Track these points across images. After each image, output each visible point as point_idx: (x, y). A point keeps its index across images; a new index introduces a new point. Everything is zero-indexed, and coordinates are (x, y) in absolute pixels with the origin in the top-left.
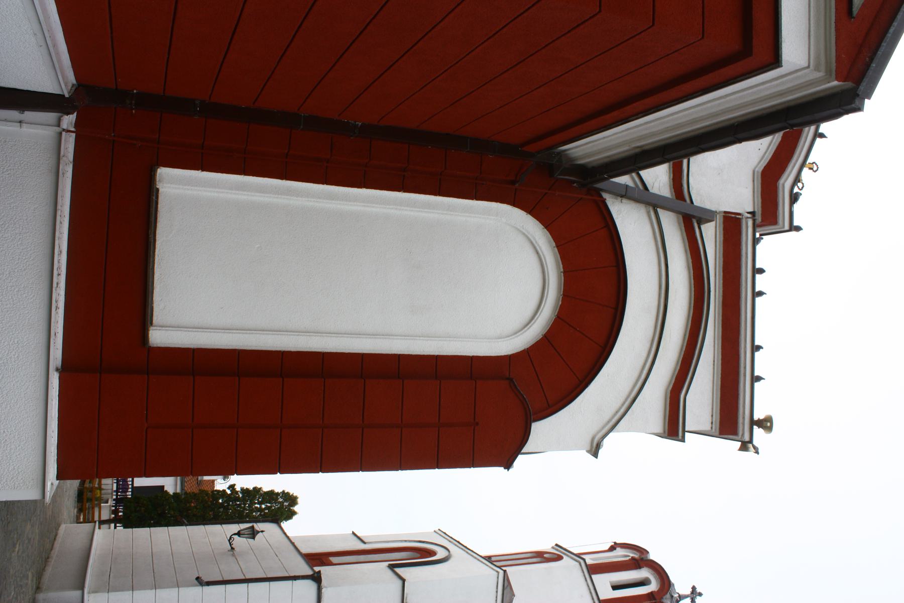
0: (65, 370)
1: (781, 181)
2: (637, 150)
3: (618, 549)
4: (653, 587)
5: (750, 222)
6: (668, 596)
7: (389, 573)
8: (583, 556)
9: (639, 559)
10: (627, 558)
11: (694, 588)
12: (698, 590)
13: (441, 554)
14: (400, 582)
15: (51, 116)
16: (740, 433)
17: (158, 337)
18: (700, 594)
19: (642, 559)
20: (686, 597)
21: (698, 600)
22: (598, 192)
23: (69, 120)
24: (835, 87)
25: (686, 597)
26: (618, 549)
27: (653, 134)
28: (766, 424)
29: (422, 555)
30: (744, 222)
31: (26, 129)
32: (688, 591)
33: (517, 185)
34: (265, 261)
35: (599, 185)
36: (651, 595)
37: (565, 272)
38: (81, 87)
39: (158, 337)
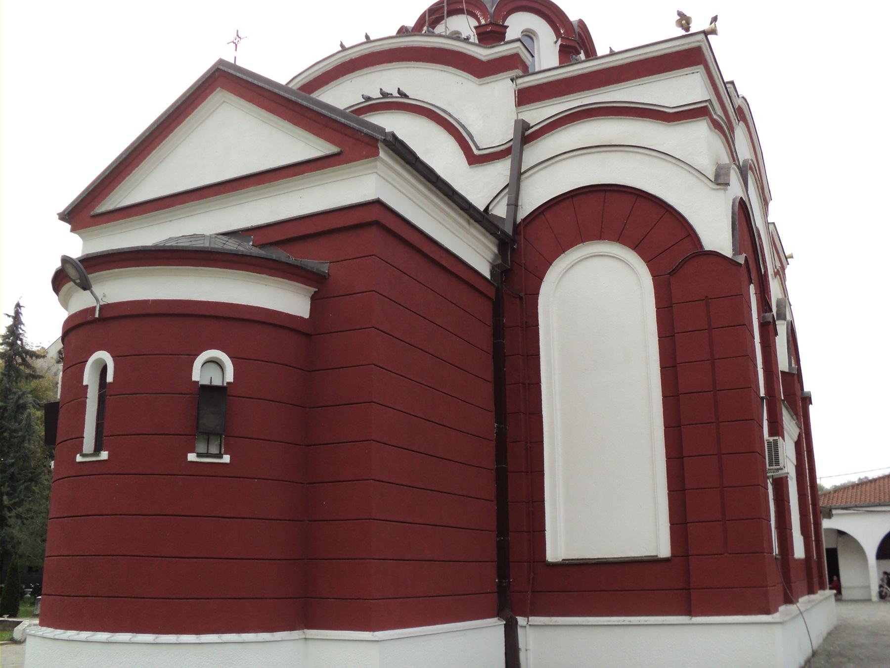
0: (690, 613)
1: (484, 59)
2: (472, 221)
5: (520, 81)
15: (520, 632)
16: (697, 44)
17: (664, 550)
22: (516, 227)
23: (521, 620)
24: (385, 151)
27: (455, 221)
28: (684, 21)
30: (520, 87)
31: (531, 646)
33: (522, 294)
35: (509, 229)
37: (583, 242)
38: (499, 614)
39: (664, 550)
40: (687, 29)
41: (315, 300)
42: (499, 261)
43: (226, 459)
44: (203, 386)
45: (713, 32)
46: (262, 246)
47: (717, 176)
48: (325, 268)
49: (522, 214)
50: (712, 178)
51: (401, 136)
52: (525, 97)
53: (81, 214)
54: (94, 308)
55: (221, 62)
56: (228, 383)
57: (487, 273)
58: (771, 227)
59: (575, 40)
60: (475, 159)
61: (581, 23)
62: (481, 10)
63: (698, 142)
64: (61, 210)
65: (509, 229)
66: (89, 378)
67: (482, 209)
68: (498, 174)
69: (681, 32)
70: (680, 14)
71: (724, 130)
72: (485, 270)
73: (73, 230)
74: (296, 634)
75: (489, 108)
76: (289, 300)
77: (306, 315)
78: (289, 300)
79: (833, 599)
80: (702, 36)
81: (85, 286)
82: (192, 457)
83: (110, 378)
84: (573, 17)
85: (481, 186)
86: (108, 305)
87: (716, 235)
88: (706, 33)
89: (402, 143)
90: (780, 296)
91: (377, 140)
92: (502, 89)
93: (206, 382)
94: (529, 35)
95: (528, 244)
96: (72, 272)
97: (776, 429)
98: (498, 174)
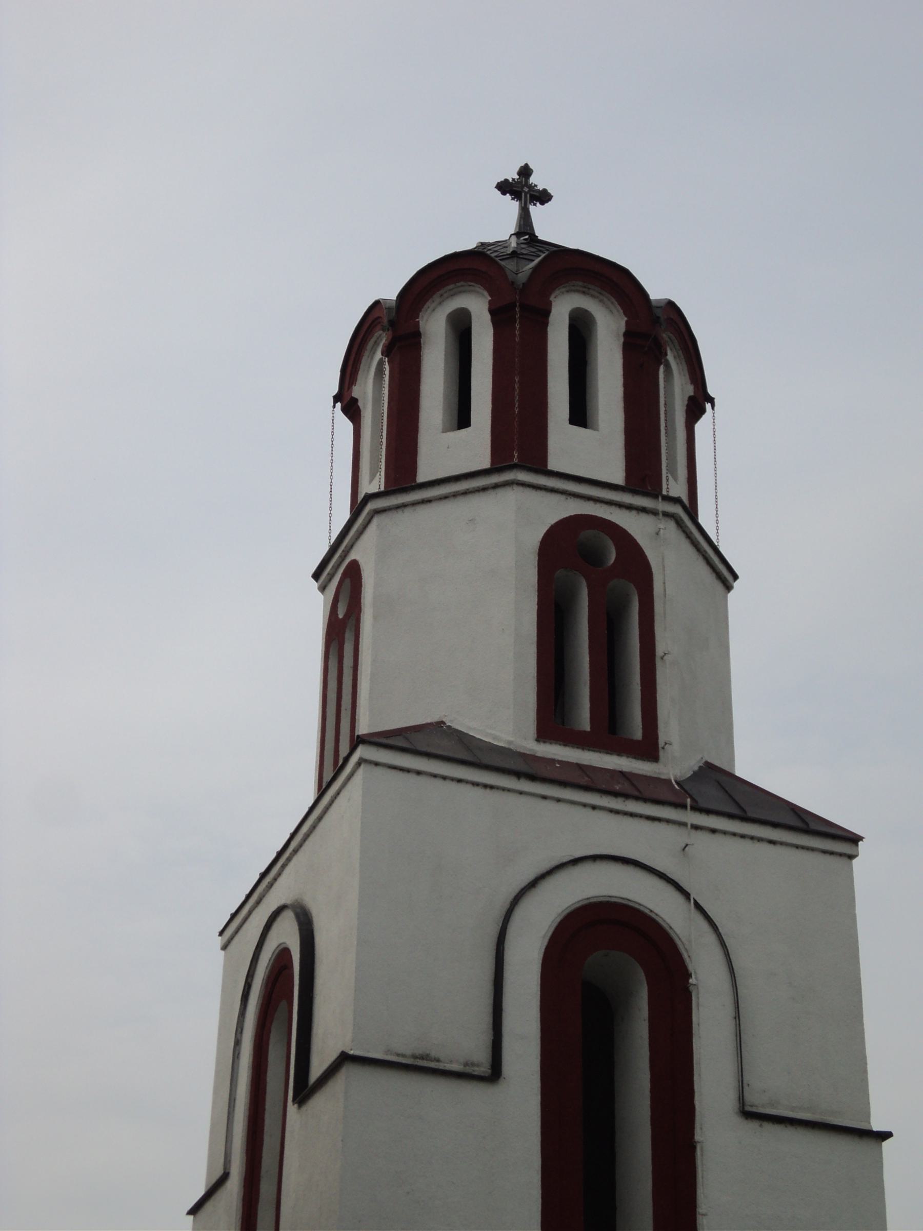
3: (356, 392)
4: (477, 305)
6: (510, 265)
7: (319, 1102)
8: (361, 497)
9: (389, 333)
10: (387, 367)
11: (504, 187)
12: (512, 175)
13: (286, 934)
14: (347, 1073)
18: (525, 172)
19: (392, 323)
21: (538, 180)
26: (356, 392)
29: (278, 995)
32: (510, 207)
36: (500, 316)
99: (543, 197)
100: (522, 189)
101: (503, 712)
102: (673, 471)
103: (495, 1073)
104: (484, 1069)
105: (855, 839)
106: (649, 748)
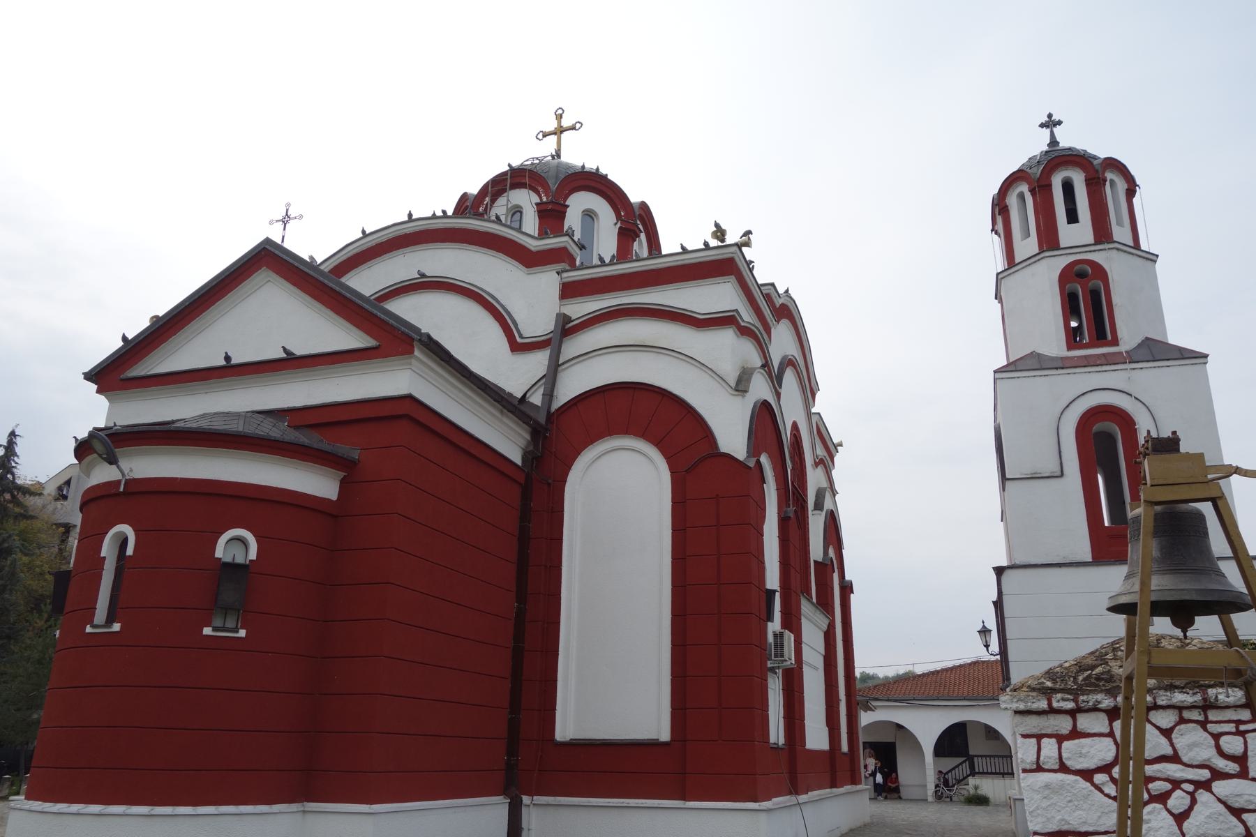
0: (684, 798)
4: (1024, 188)
5: (565, 275)
9: (1000, 207)
11: (1042, 126)
12: (1045, 119)
17: (665, 735)
20: (1052, 134)
21: (1056, 117)
22: (550, 416)
23: (526, 799)
24: (421, 351)
25: (1052, 134)
28: (720, 233)
31: (533, 827)
32: (1047, 132)
34: (615, 663)
35: (542, 419)
36: (1032, 191)
38: (504, 792)
39: (665, 735)
40: (723, 240)
41: (344, 484)
42: (531, 448)
43: (242, 633)
44: (227, 565)
45: (747, 244)
46: (296, 427)
47: (739, 381)
48: (356, 455)
49: (556, 405)
50: (733, 384)
51: (435, 336)
52: (569, 291)
53: (110, 376)
54: (119, 482)
55: (267, 241)
56: (251, 561)
57: (518, 461)
58: (814, 419)
59: (636, 222)
60: (518, 346)
61: (644, 206)
62: (543, 187)
63: (726, 350)
64: (87, 370)
65: (542, 419)
66: (107, 549)
67: (519, 396)
68: (538, 362)
69: (714, 243)
70: (717, 225)
71: (757, 336)
72: (516, 457)
73: (98, 392)
74: (294, 807)
75: (534, 298)
76: (318, 484)
77: (334, 498)
78: (318, 484)
79: (866, 796)
80: (735, 248)
81: (112, 460)
82: (207, 631)
83: (130, 551)
84: (634, 198)
85: (518, 375)
86: (134, 480)
87: (732, 435)
88: (739, 246)
89: (437, 344)
90: (825, 484)
91: (413, 339)
92: (548, 281)
93: (228, 559)
94: (589, 215)
95: (560, 432)
96: (98, 446)
97: (792, 621)
98: (538, 362)
99: (1059, 123)
100: (1051, 123)
101: (1055, 345)
102: (1120, 223)
103: (1062, 475)
104: (1059, 473)
105: (1206, 356)
106: (1115, 342)
